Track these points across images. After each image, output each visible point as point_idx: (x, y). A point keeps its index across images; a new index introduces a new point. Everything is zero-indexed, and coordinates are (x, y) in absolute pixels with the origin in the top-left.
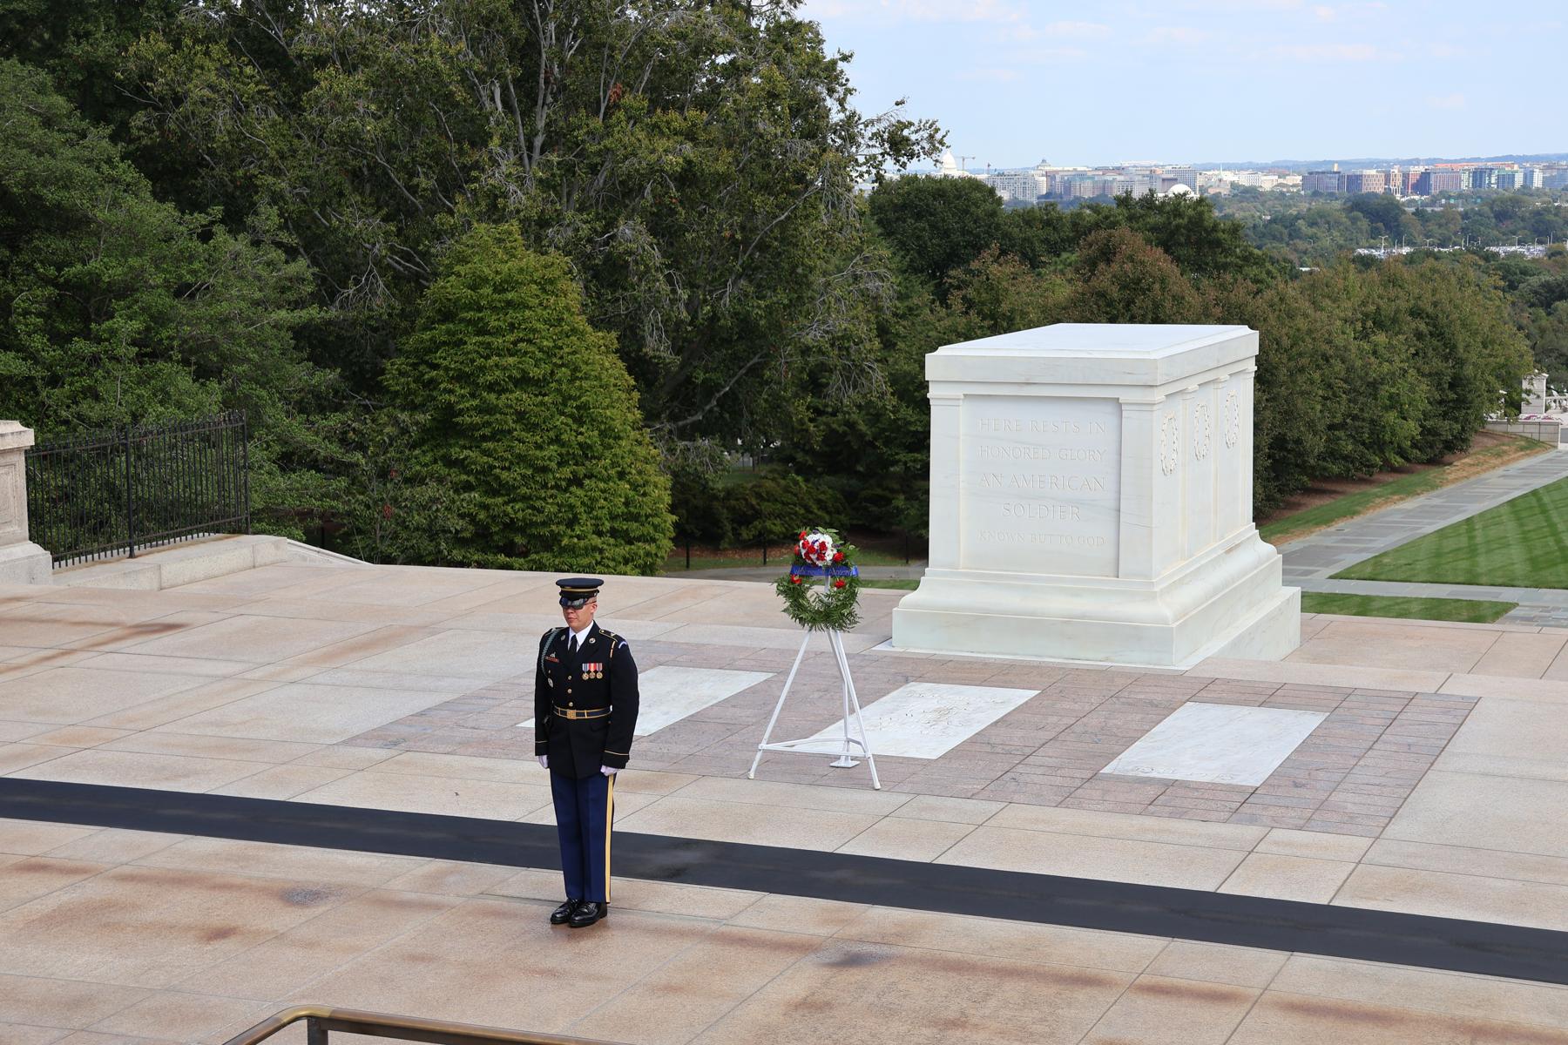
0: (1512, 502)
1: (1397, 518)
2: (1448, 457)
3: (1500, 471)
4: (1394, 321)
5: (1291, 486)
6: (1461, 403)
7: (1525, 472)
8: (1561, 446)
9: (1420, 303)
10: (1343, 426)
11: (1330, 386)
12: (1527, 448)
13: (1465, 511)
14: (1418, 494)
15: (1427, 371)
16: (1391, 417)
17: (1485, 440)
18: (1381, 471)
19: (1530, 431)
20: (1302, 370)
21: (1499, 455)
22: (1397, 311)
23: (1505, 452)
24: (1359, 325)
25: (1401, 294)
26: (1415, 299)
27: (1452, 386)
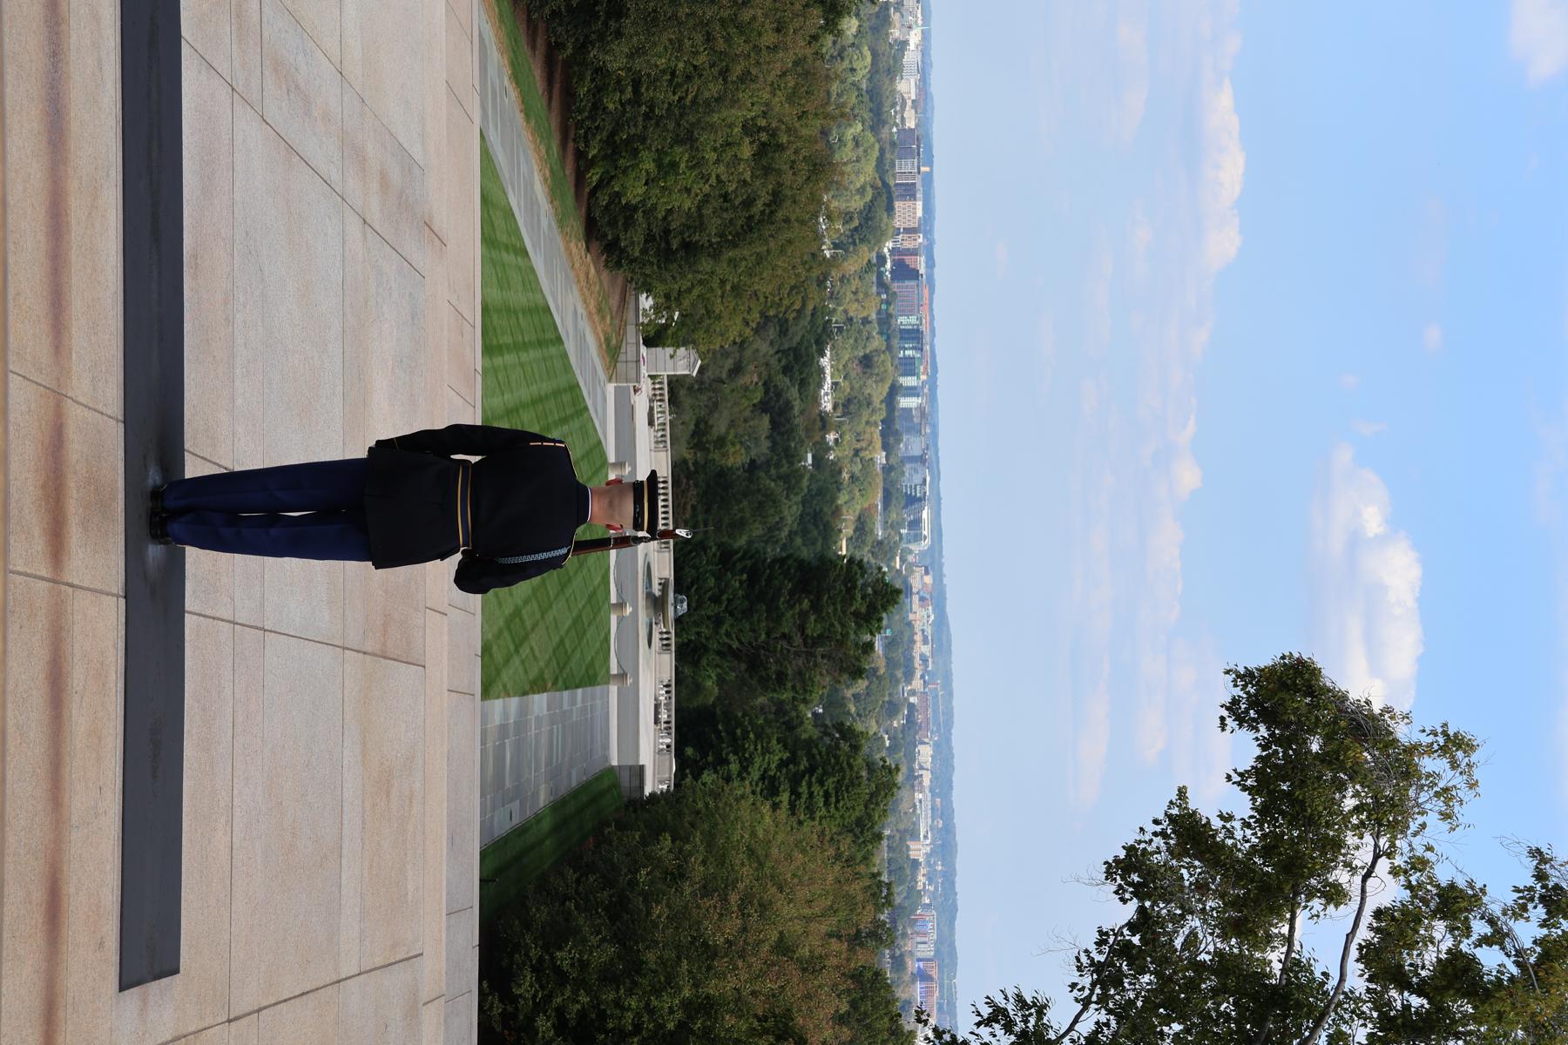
0: (547, 310)
1: (523, 168)
2: (596, 245)
3: (581, 310)
4: (767, 170)
5: (560, 29)
6: (667, 256)
7: (581, 340)
8: (611, 388)
9: (789, 203)
10: (636, 100)
11: (689, 78)
12: (608, 345)
13: (536, 252)
14: (552, 202)
15: (704, 212)
16: (649, 165)
17: (617, 297)
18: (580, 155)
19: (628, 351)
20: (709, 38)
21: (600, 310)
22: (779, 172)
23: (603, 318)
24: (762, 122)
25: (800, 180)
26: (793, 196)
27: (687, 246)
